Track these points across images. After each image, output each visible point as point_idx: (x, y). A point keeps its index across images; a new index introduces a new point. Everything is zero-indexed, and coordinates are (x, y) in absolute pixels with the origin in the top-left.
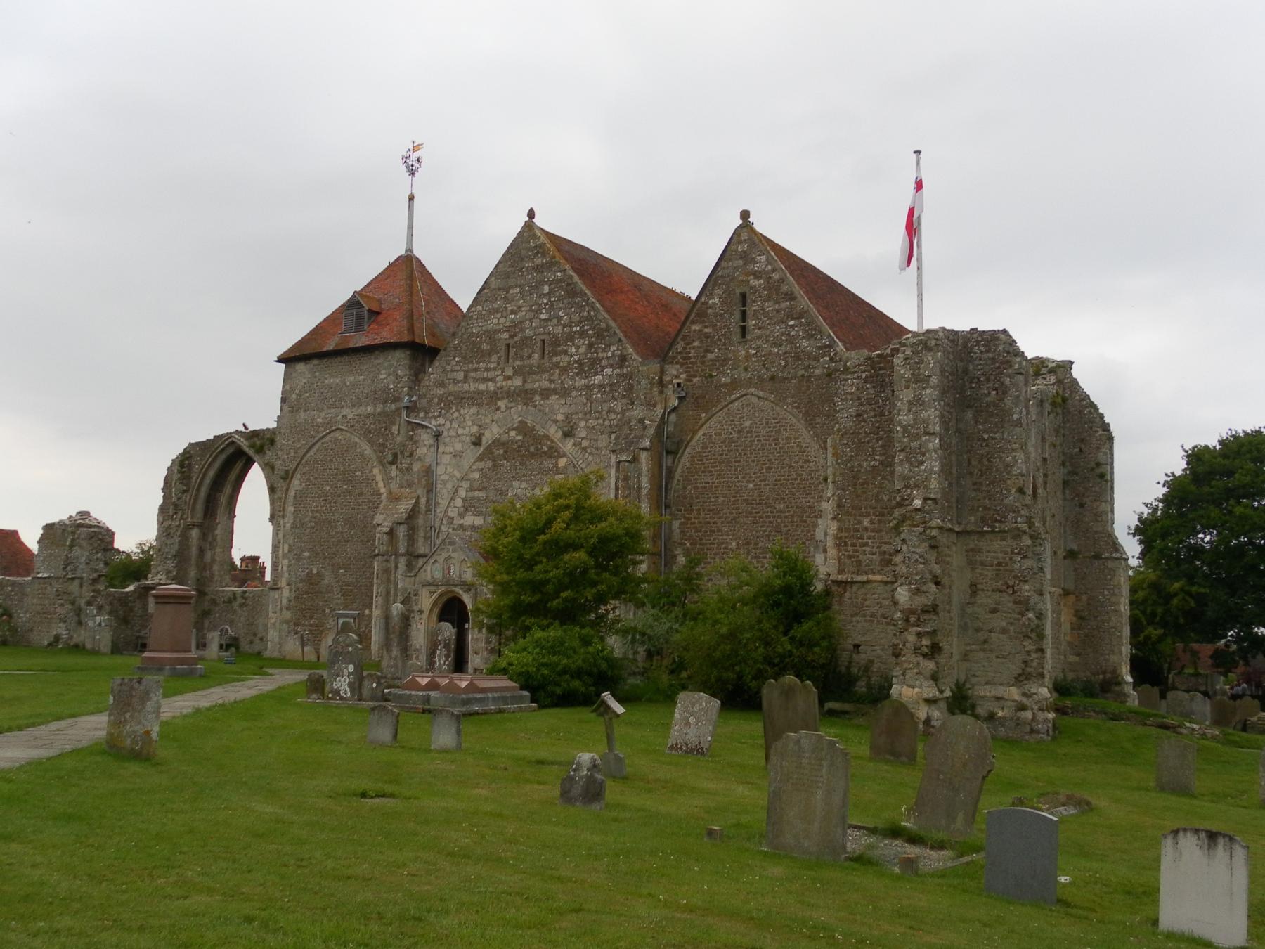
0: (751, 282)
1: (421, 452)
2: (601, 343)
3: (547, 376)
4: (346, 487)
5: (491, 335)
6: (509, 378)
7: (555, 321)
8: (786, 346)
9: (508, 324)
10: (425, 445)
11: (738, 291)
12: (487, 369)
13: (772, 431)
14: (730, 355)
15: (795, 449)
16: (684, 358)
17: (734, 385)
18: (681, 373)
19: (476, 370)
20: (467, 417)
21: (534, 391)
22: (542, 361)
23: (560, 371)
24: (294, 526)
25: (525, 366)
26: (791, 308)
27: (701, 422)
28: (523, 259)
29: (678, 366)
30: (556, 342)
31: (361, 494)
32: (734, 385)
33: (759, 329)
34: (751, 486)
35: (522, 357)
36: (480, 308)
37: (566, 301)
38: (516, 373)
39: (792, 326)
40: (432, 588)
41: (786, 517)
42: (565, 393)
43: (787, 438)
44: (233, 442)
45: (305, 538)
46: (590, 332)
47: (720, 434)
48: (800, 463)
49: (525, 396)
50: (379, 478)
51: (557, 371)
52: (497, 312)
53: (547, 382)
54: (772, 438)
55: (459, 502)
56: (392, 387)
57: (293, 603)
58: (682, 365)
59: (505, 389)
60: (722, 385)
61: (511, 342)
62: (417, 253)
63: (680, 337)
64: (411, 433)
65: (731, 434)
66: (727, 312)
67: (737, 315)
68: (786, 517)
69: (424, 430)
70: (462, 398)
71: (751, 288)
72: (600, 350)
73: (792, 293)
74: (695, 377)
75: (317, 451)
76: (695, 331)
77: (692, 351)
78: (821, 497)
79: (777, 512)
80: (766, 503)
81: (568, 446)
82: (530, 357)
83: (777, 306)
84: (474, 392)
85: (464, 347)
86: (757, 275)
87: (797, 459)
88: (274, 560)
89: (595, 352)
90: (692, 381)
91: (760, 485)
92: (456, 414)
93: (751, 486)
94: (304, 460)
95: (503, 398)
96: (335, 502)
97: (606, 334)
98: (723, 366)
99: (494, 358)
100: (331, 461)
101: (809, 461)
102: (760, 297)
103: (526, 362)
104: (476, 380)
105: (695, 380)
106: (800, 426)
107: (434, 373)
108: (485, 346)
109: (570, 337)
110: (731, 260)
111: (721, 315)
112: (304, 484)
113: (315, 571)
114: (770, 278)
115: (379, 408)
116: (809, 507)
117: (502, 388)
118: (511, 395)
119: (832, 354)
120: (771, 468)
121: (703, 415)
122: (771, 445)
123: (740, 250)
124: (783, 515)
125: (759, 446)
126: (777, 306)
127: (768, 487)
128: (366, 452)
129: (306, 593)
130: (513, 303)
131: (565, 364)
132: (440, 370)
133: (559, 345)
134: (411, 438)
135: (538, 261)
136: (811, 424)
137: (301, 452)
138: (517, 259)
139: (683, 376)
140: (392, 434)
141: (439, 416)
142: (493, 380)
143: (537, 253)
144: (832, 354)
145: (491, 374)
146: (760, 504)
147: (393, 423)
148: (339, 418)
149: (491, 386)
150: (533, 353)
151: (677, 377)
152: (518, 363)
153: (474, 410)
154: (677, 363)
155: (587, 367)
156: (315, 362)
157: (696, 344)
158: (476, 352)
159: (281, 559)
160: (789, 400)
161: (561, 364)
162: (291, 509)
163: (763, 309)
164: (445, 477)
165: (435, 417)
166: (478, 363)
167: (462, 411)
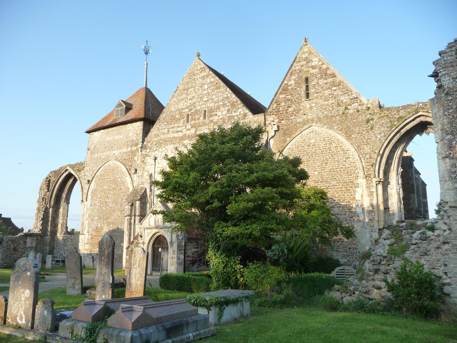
0: (311, 71)
1: (148, 167)
2: (234, 109)
3: (207, 127)
4: (114, 186)
5: (180, 111)
6: (189, 130)
7: (211, 101)
8: (332, 100)
9: (188, 105)
10: (150, 164)
11: (304, 76)
12: (178, 127)
13: (326, 144)
14: (301, 108)
15: (341, 152)
16: (277, 112)
17: (305, 122)
18: (276, 119)
19: (173, 127)
20: (169, 150)
22: (205, 120)
23: (214, 124)
24: (91, 205)
25: (196, 123)
26: (334, 82)
27: (287, 142)
28: (195, 75)
29: (274, 116)
30: (211, 111)
31: (120, 189)
32: (305, 122)
33: (317, 93)
34: (316, 173)
35: (195, 119)
36: (175, 99)
37: (215, 91)
38: (192, 127)
39: (335, 90)
40: (149, 231)
41: (338, 188)
43: (336, 147)
44: (67, 170)
45: (96, 211)
46: (228, 104)
47: (298, 148)
48: (344, 159)
51: (212, 124)
52: (183, 100)
53: (207, 130)
54: (327, 147)
56: (135, 139)
57: (90, 241)
58: (276, 115)
59: (187, 135)
60: (298, 123)
61: (190, 113)
62: (148, 87)
63: (274, 101)
64: (143, 159)
65: (304, 147)
66: (298, 87)
67: (304, 87)
68: (338, 188)
69: (149, 157)
70: (167, 141)
71: (311, 74)
72: (233, 112)
73: (334, 74)
74: (283, 120)
75: (102, 170)
76: (282, 98)
77: (281, 108)
78: (358, 176)
79: (332, 186)
80: (326, 181)
82: (198, 119)
83: (325, 81)
84: (173, 138)
85: (168, 118)
86: (313, 67)
87: (342, 157)
88: (82, 221)
89: (231, 113)
90: (281, 122)
91: (321, 172)
92: (164, 149)
93: (316, 173)
94: (96, 175)
95: (186, 139)
96: (109, 194)
97: (236, 104)
98: (297, 113)
99: (182, 121)
100: (108, 174)
101: (349, 158)
102: (316, 78)
103: (197, 121)
104: (173, 132)
105: (283, 122)
106: (342, 139)
107: (154, 130)
108: (177, 116)
109: (218, 108)
110: (299, 62)
111: (295, 89)
112: (96, 186)
113: (99, 226)
114: (321, 68)
115: (129, 149)
116: (350, 182)
117: (185, 135)
119: (359, 101)
120: (328, 163)
121: (288, 139)
122: (326, 151)
123: (304, 56)
124: (336, 187)
125: (320, 152)
126: (325, 81)
127: (326, 173)
128: (123, 170)
129: (96, 236)
130: (190, 95)
131: (216, 120)
132: (157, 129)
133: (213, 112)
134: (143, 162)
135: (202, 75)
136: (349, 138)
137: (95, 172)
138: (192, 75)
139: (277, 121)
140: (135, 161)
141: (156, 150)
142: (181, 131)
143: (202, 71)
144: (359, 101)
145: (179, 129)
146: (321, 182)
147: (136, 156)
148: (111, 155)
149: (180, 134)
150: (200, 117)
151: (273, 121)
152: (193, 122)
154: (273, 114)
156: (102, 131)
157: (282, 104)
158: (174, 119)
159: (85, 220)
160: (336, 127)
161: (214, 121)
162: (89, 197)
163: (318, 84)
165: (154, 151)
166: (174, 124)
167: (167, 147)
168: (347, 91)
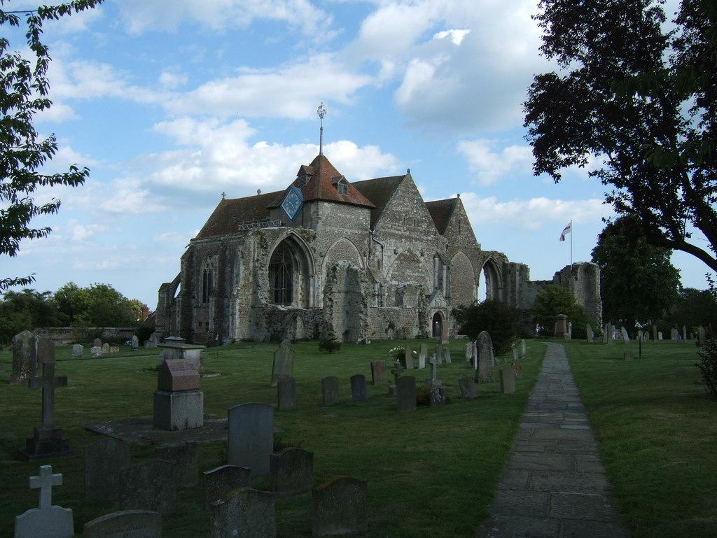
21: (412, 238)
42: (421, 240)
49: (409, 239)
50: (360, 261)
55: (390, 275)
81: (422, 259)
99: (401, 222)
104: (395, 229)
107: (380, 223)
118: (406, 237)
142: (400, 230)
149: (400, 233)
153: (394, 240)
155: (427, 233)
164: (385, 265)
168: (473, 236)
